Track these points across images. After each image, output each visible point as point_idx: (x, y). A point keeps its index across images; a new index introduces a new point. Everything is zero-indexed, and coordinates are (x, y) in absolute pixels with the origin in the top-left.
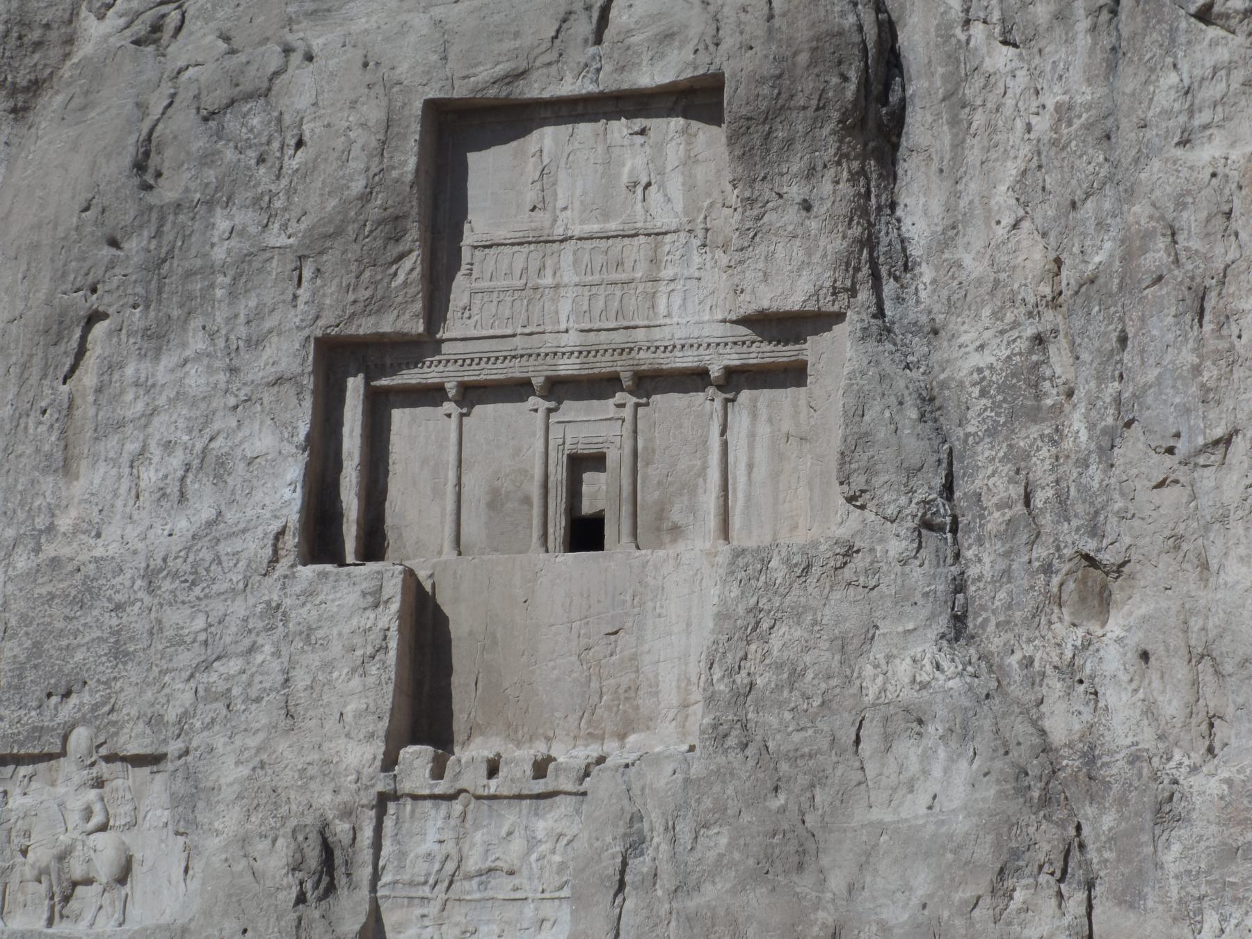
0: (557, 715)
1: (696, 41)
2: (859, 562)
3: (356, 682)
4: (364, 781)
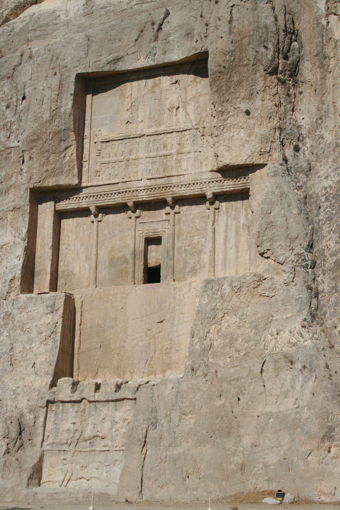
1: (197, 36)
2: (266, 284)
3: (42, 348)
4: (41, 395)
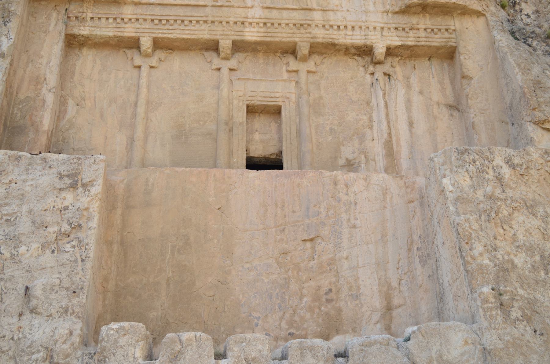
0: (255, 314)
3: (48, 259)
